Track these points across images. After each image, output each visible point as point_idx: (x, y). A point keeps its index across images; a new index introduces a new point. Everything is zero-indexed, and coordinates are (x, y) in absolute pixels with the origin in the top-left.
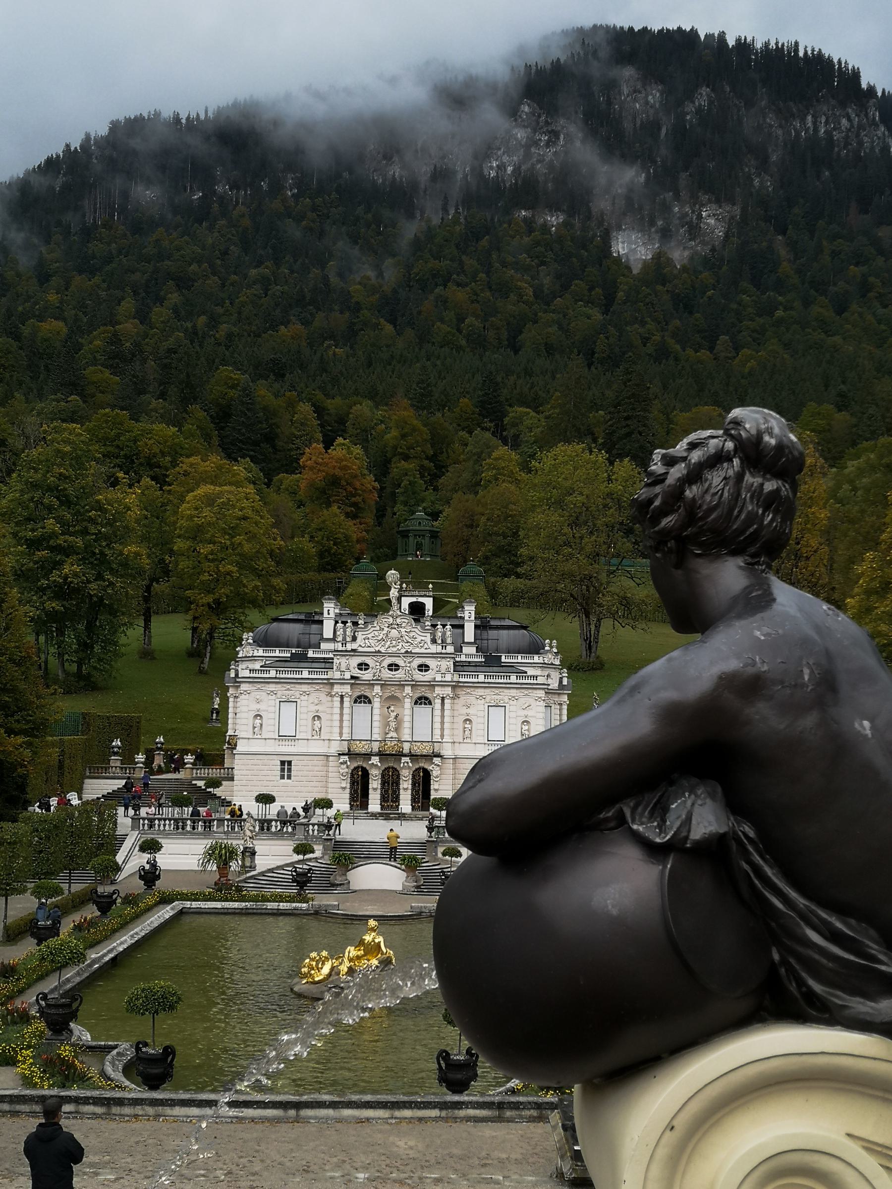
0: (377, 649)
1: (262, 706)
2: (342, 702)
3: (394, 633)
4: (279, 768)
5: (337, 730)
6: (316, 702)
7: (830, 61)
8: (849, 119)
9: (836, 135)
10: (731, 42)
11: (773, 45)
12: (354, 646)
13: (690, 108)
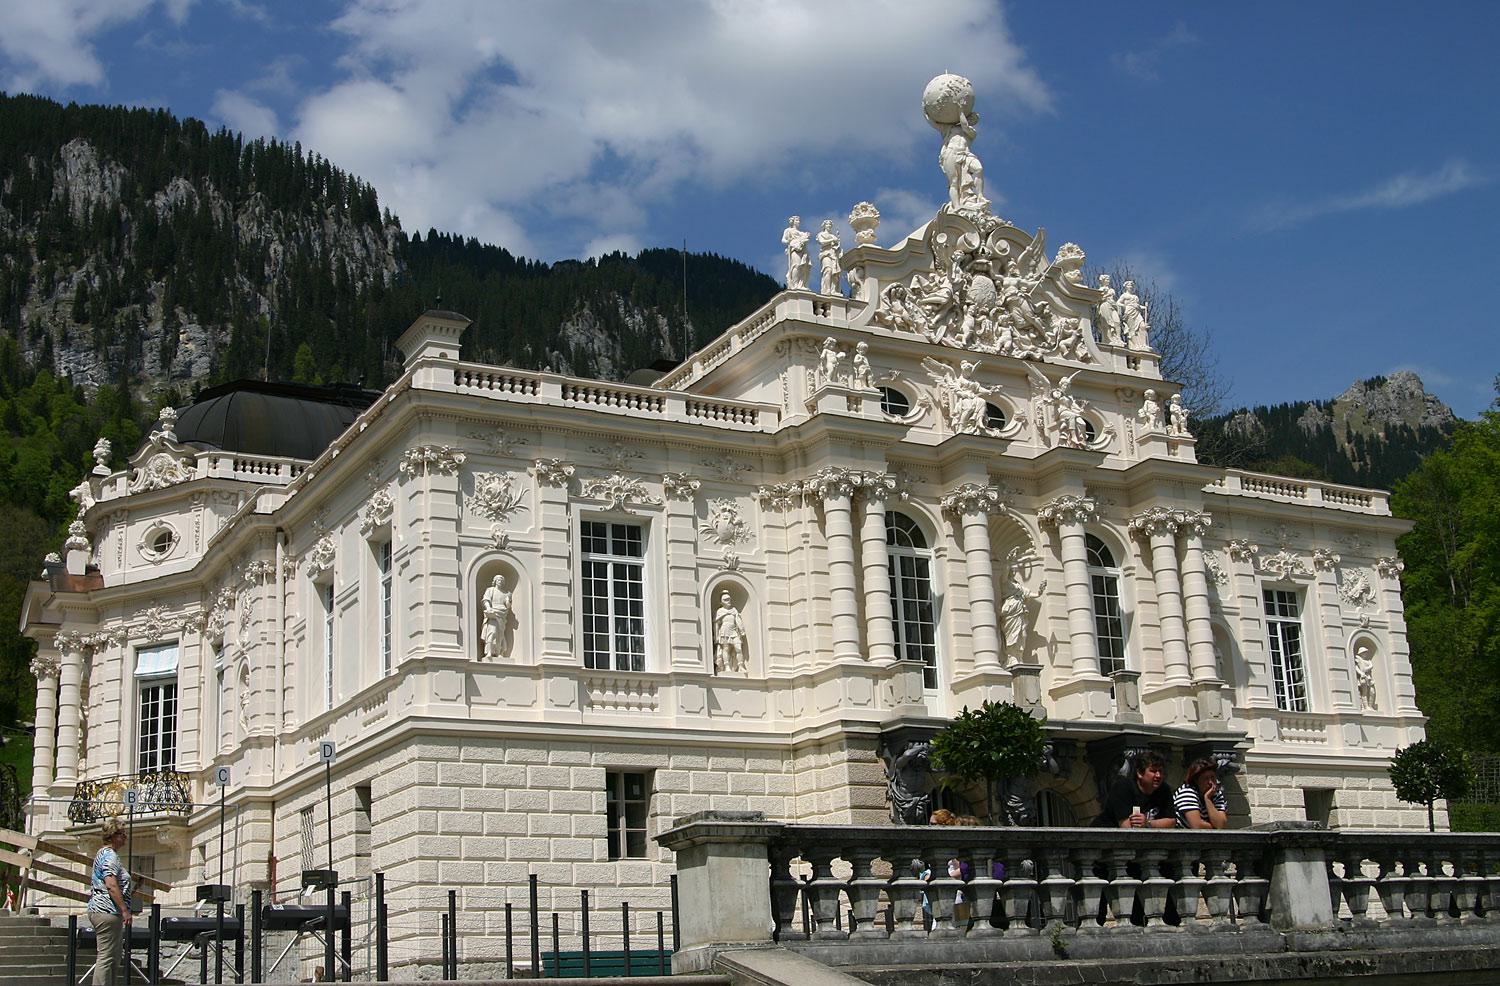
0: (937, 337)
1: (516, 529)
2: (856, 518)
3: (980, 285)
4: (600, 800)
5: (846, 629)
6: (723, 523)
7: (338, 176)
8: (365, 245)
9: (351, 267)
10: (212, 130)
11: (267, 144)
12: (858, 320)
13: (160, 200)
